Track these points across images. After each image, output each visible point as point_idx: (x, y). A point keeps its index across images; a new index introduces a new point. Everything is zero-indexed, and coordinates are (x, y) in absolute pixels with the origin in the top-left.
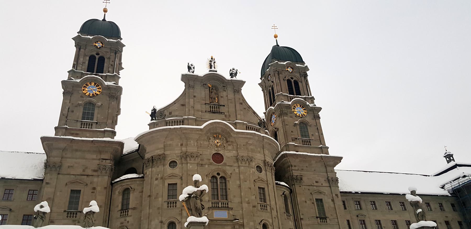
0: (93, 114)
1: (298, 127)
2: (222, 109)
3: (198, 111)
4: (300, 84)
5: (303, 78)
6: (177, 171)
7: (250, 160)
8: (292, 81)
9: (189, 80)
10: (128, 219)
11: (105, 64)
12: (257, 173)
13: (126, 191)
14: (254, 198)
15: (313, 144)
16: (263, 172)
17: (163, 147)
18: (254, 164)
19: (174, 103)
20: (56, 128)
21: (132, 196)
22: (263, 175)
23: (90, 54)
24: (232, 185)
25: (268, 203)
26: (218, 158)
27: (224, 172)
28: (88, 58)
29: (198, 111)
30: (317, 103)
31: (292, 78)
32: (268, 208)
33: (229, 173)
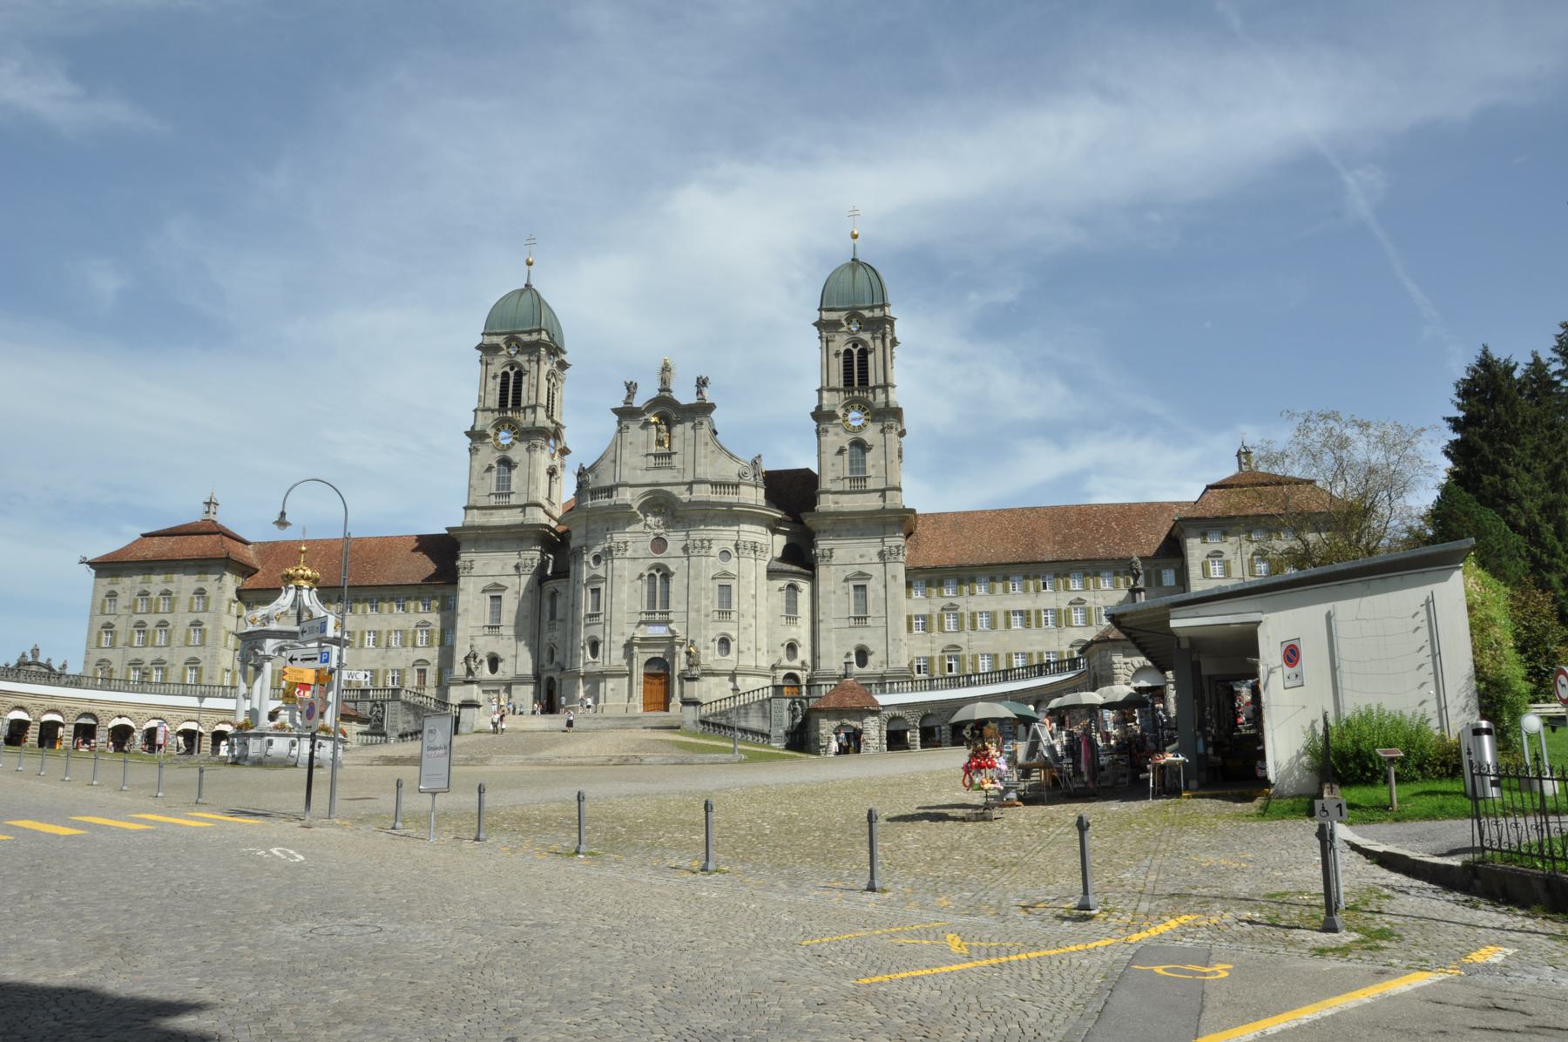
0: (509, 479)
1: (846, 455)
2: (676, 460)
3: (635, 468)
4: (871, 357)
5: (878, 342)
6: (600, 571)
7: (706, 545)
8: (855, 351)
9: (626, 414)
10: (556, 634)
11: (524, 387)
12: (719, 563)
13: (554, 595)
14: (709, 601)
15: (871, 484)
16: (734, 560)
17: (583, 532)
18: (715, 550)
19: (601, 458)
20: (466, 508)
21: (559, 602)
22: (731, 566)
23: (500, 373)
24: (675, 584)
25: (734, 607)
26: (659, 544)
27: (666, 567)
28: (499, 380)
29: (635, 468)
30: (896, 397)
31: (855, 346)
32: (734, 616)
33: (672, 569)
